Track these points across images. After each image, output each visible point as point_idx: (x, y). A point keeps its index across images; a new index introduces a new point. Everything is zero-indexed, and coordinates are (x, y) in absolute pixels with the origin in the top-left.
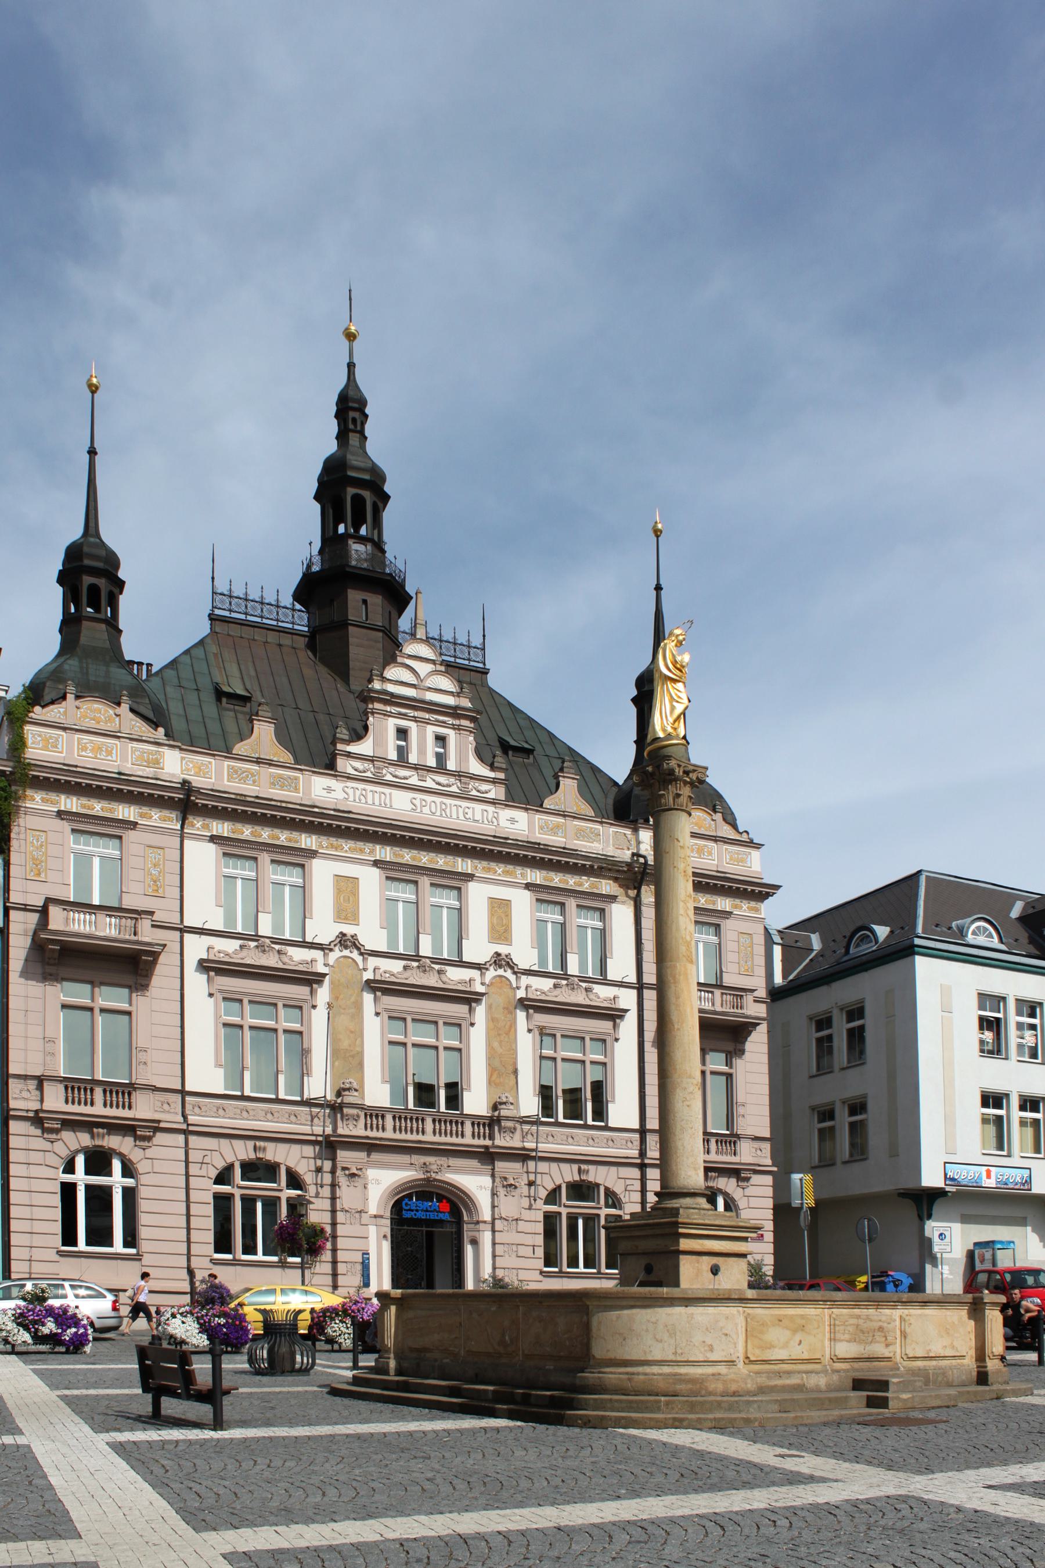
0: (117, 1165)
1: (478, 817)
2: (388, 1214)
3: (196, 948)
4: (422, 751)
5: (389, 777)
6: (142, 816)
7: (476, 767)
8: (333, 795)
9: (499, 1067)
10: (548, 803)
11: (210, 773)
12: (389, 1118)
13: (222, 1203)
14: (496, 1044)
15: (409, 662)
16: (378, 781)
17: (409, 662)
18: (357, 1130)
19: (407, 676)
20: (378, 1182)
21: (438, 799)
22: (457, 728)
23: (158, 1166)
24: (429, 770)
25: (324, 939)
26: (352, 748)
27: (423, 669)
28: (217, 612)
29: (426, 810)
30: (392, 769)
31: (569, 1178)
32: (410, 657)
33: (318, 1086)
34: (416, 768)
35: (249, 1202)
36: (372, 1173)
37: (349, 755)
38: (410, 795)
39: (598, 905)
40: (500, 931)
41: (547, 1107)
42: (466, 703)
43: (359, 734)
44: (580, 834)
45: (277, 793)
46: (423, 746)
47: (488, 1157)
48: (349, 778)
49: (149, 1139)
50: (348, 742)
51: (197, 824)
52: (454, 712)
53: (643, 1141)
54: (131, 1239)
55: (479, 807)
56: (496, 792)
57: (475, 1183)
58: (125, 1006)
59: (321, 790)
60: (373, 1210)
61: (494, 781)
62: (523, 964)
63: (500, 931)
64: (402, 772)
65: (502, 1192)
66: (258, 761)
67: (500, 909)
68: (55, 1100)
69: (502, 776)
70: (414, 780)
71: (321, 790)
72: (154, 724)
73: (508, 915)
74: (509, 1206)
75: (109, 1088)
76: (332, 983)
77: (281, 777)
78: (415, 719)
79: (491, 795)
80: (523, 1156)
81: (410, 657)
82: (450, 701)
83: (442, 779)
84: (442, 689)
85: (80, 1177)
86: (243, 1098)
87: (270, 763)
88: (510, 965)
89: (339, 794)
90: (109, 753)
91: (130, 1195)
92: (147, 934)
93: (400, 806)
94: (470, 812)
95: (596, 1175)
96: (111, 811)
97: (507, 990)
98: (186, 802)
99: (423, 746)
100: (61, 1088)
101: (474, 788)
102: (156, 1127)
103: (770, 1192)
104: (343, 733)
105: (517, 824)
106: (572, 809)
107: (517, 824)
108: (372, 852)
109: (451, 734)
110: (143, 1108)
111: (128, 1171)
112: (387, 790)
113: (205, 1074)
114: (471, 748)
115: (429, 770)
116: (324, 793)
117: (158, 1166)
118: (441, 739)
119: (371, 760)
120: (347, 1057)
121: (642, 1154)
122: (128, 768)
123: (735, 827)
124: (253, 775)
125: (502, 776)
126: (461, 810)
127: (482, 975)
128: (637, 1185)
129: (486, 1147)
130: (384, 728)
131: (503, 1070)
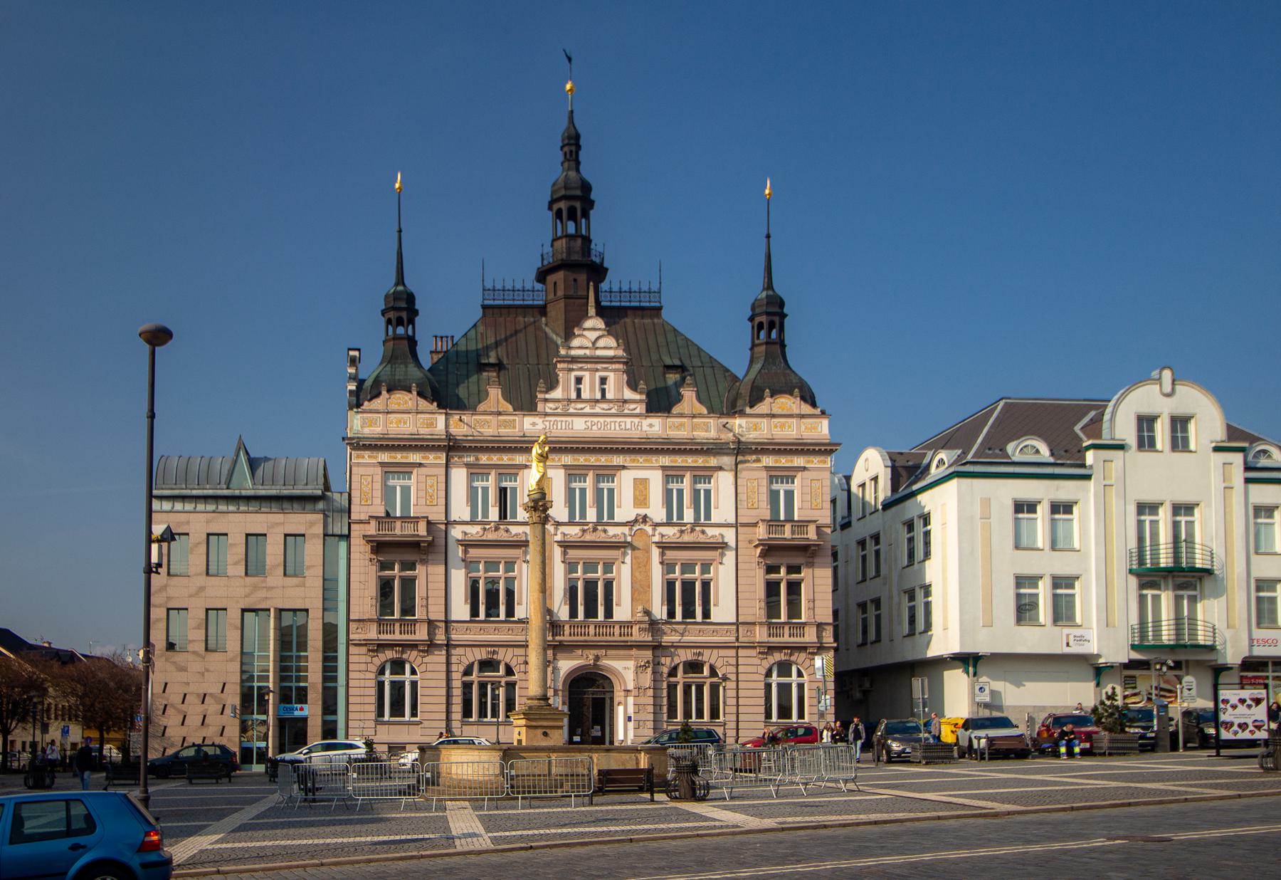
0: (407, 667)
5: (571, 410)
7: (628, 394)
13: (467, 687)
17: (585, 333)
21: (602, 420)
22: (614, 370)
24: (597, 401)
26: (547, 396)
27: (593, 335)
35: (483, 686)
37: (546, 400)
38: (583, 419)
40: (641, 498)
43: (552, 385)
48: (546, 415)
50: (546, 392)
52: (611, 360)
54: (414, 714)
55: (629, 420)
62: (657, 520)
63: (641, 498)
64: (580, 406)
70: (588, 410)
71: (530, 425)
79: (638, 411)
82: (611, 353)
83: (605, 406)
84: (609, 346)
87: (499, 414)
89: (540, 426)
91: (414, 684)
93: (579, 427)
107: (654, 426)
111: (413, 672)
112: (569, 419)
115: (597, 401)
123: (814, 405)
128: (733, 661)
130: (566, 379)
131: (640, 589)
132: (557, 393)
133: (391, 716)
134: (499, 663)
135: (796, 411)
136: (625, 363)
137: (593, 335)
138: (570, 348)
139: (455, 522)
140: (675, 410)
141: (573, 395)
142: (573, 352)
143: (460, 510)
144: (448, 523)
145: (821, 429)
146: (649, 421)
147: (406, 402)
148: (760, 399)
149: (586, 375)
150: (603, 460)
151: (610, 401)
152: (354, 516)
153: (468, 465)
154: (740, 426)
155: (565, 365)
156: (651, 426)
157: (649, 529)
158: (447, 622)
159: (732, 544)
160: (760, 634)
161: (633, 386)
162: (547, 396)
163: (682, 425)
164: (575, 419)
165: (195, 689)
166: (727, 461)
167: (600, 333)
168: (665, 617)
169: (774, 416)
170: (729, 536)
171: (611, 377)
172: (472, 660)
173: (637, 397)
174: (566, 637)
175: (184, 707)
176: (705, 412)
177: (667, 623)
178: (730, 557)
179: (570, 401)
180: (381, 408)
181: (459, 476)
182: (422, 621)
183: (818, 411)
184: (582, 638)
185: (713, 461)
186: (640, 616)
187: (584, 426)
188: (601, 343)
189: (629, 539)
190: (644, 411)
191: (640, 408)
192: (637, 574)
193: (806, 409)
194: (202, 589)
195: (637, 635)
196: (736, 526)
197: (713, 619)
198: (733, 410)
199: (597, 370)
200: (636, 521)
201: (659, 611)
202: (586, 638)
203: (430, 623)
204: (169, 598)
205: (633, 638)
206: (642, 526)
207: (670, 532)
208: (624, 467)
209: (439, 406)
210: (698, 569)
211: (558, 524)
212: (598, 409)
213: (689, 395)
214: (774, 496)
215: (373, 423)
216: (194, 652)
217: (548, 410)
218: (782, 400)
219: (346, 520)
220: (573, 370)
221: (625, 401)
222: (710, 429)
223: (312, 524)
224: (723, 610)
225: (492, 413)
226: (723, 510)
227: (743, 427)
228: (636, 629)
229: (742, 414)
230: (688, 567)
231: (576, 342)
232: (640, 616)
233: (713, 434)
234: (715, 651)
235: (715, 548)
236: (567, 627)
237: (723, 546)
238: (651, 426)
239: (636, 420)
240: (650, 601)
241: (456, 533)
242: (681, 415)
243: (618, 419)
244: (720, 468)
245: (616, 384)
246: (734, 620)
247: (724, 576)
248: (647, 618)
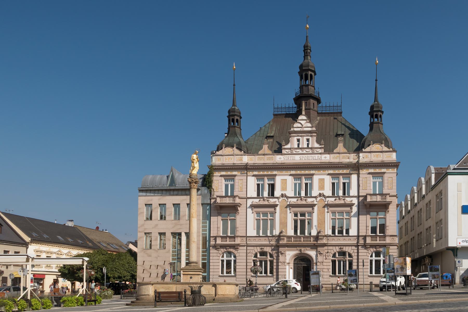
1: (316, 158)
2: (292, 262)
3: (250, 202)
5: (294, 152)
7: (316, 145)
9: (322, 222)
12: (293, 238)
14: (320, 217)
15: (300, 121)
17: (300, 121)
18: (284, 241)
19: (300, 125)
20: (289, 255)
21: (306, 156)
23: (241, 254)
26: (285, 147)
27: (303, 122)
28: (275, 113)
31: (338, 250)
32: (300, 120)
33: (276, 232)
34: (301, 149)
36: (287, 253)
39: (348, 176)
40: (322, 187)
41: (334, 232)
42: (314, 129)
44: (344, 158)
47: (314, 247)
49: (238, 248)
51: (250, 173)
53: (358, 239)
55: (316, 155)
56: (322, 151)
57: (312, 253)
58: (233, 218)
59: (279, 159)
60: (287, 261)
61: (321, 148)
63: (322, 187)
65: (319, 255)
66: (264, 155)
67: (322, 181)
68: (219, 241)
69: (323, 146)
71: (279, 159)
72: (241, 150)
73: (324, 183)
74: (320, 259)
75: (230, 237)
76: (280, 206)
78: (301, 136)
79: (320, 152)
80: (324, 245)
81: (300, 120)
82: (310, 129)
83: (307, 150)
85: (374, 258)
86: (259, 236)
87: (267, 155)
88: (324, 196)
89: (283, 159)
90: (232, 159)
91: (235, 261)
92: (238, 201)
93: (297, 159)
95: (346, 249)
97: (323, 202)
98: (246, 168)
100: (220, 238)
102: (238, 245)
103: (390, 251)
105: (327, 158)
106: (342, 151)
109: (310, 138)
110: (238, 241)
111: (235, 257)
112: (294, 156)
113: (252, 232)
114: (315, 140)
117: (241, 254)
118: (308, 140)
119: (290, 149)
120: (284, 224)
121: (358, 242)
122: (235, 162)
125: (323, 146)
127: (316, 199)
129: (314, 244)
132: (288, 146)
133: (226, 273)
134: (266, 252)
140: (335, 151)
142: (295, 129)
145: (393, 157)
156: (325, 157)
160: (369, 240)
161: (318, 142)
162: (285, 147)
163: (338, 157)
164: (296, 156)
165: (154, 263)
172: (256, 251)
175: (150, 270)
183: (391, 149)
184: (297, 243)
191: (322, 151)
193: (386, 149)
194: (157, 225)
197: (350, 235)
198: (358, 150)
199: (304, 136)
202: (300, 242)
204: (145, 229)
209: (244, 152)
213: (341, 145)
215: (219, 160)
216: (154, 250)
218: (378, 145)
227: (364, 157)
230: (303, 215)
231: (296, 125)
238: (325, 157)
239: (320, 155)
243: (313, 155)
246: (356, 234)
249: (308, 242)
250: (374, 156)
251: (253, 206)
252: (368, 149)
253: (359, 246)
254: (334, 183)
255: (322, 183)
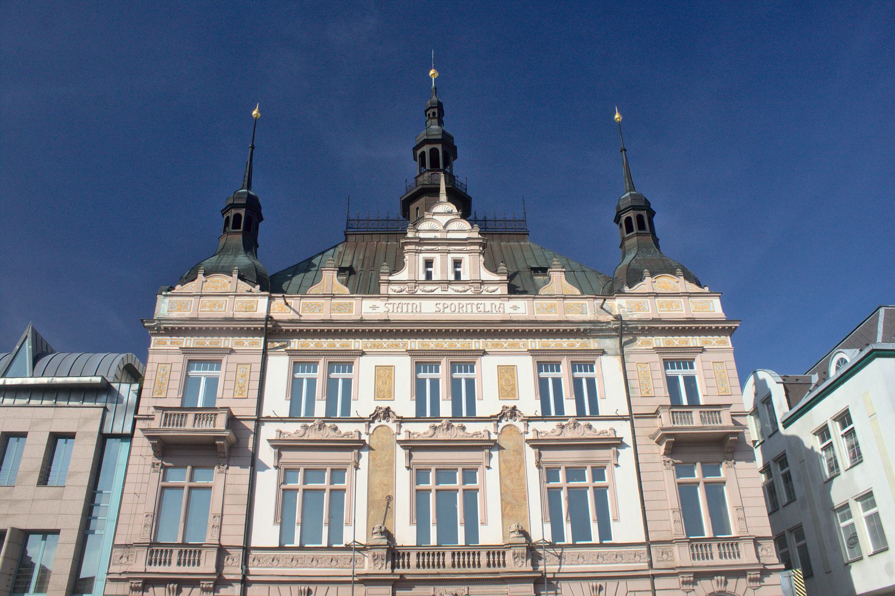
1: (488, 308)
4: (444, 270)
5: (419, 292)
6: (237, 344)
7: (486, 275)
8: (377, 310)
10: (542, 292)
11: (282, 309)
16: (413, 296)
24: (449, 283)
25: (366, 413)
26: (391, 278)
29: (447, 310)
30: (421, 287)
32: (434, 214)
38: (434, 302)
43: (397, 266)
45: (336, 316)
46: (442, 269)
48: (389, 297)
50: (391, 275)
55: (488, 303)
59: (370, 308)
64: (429, 288)
70: (439, 291)
71: (370, 308)
77: (340, 304)
79: (498, 292)
82: (464, 236)
83: (460, 288)
87: (333, 296)
93: (428, 310)
94: (482, 307)
96: (217, 343)
99: (442, 269)
101: (486, 290)
104: (385, 269)
105: (520, 309)
107: (520, 309)
108: (405, 345)
112: (417, 302)
115: (449, 283)
116: (370, 310)
118: (457, 263)
124: (319, 306)
126: (474, 307)
132: (403, 275)
135: (681, 290)
136: (480, 244)
137: (444, 219)
138: (418, 231)
139: (270, 419)
141: (422, 277)
142: (422, 235)
143: (277, 402)
144: (259, 421)
146: (513, 302)
147: (224, 285)
148: (640, 279)
149: (437, 258)
150: (459, 344)
151: (466, 283)
152: (141, 412)
153: (291, 353)
154: (620, 306)
155: (413, 247)
157: (520, 426)
158: (247, 549)
159: (628, 440)
161: (492, 266)
162: (391, 278)
163: (552, 306)
166: (611, 344)
167: (453, 217)
168: (549, 538)
169: (657, 295)
170: (623, 430)
171: (466, 259)
173: (496, 278)
174: (411, 569)
176: (578, 293)
177: (552, 545)
178: (626, 456)
179: (417, 282)
180: (194, 292)
181: (279, 366)
182: (210, 546)
183: (706, 289)
184: (436, 570)
185: (593, 344)
186: (514, 538)
187: (434, 309)
188: (453, 226)
189: (494, 437)
190: (506, 293)
191: (503, 289)
192: (508, 482)
193: (693, 288)
195: (515, 564)
196: (631, 418)
197: (615, 539)
198: (612, 290)
199: (449, 252)
200: (502, 416)
201: (540, 531)
203: (222, 551)
205: (507, 569)
206: (510, 422)
207: (548, 429)
208: (484, 353)
210: (588, 473)
211: (401, 420)
212: (451, 291)
214: (672, 383)
217: (391, 292)
219: (130, 417)
220: (421, 252)
221: (482, 283)
222: (587, 310)
223: (87, 420)
224: (627, 527)
225: (324, 296)
226: (612, 400)
228: (509, 554)
229: (621, 293)
231: (424, 226)
232: (514, 538)
233: (589, 316)
234: (622, 583)
235: (607, 446)
236: (413, 556)
237: (618, 444)
238: (515, 308)
239: (497, 302)
240: (527, 517)
241: (268, 432)
242: (550, 297)
243: (476, 302)
244: (603, 352)
245: (473, 265)
247: (622, 479)
248: (523, 540)
249: (472, 570)
250: (661, 306)
251: (281, 446)
252: (639, 288)
253: (653, 576)
254: (546, 379)
255: (505, 379)
